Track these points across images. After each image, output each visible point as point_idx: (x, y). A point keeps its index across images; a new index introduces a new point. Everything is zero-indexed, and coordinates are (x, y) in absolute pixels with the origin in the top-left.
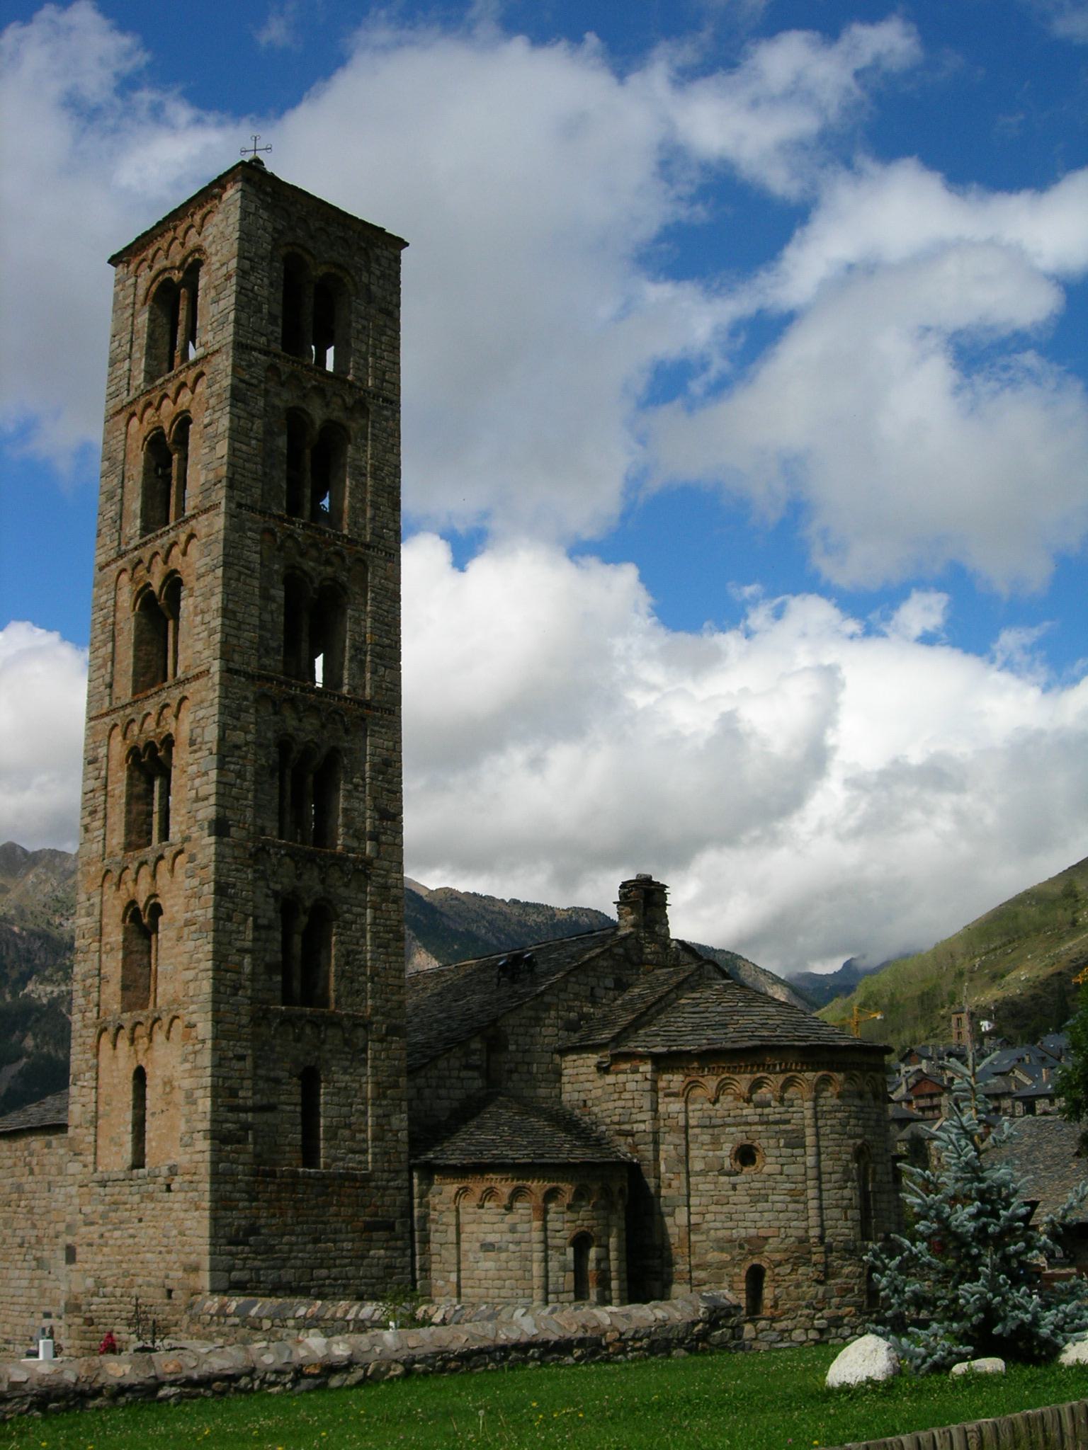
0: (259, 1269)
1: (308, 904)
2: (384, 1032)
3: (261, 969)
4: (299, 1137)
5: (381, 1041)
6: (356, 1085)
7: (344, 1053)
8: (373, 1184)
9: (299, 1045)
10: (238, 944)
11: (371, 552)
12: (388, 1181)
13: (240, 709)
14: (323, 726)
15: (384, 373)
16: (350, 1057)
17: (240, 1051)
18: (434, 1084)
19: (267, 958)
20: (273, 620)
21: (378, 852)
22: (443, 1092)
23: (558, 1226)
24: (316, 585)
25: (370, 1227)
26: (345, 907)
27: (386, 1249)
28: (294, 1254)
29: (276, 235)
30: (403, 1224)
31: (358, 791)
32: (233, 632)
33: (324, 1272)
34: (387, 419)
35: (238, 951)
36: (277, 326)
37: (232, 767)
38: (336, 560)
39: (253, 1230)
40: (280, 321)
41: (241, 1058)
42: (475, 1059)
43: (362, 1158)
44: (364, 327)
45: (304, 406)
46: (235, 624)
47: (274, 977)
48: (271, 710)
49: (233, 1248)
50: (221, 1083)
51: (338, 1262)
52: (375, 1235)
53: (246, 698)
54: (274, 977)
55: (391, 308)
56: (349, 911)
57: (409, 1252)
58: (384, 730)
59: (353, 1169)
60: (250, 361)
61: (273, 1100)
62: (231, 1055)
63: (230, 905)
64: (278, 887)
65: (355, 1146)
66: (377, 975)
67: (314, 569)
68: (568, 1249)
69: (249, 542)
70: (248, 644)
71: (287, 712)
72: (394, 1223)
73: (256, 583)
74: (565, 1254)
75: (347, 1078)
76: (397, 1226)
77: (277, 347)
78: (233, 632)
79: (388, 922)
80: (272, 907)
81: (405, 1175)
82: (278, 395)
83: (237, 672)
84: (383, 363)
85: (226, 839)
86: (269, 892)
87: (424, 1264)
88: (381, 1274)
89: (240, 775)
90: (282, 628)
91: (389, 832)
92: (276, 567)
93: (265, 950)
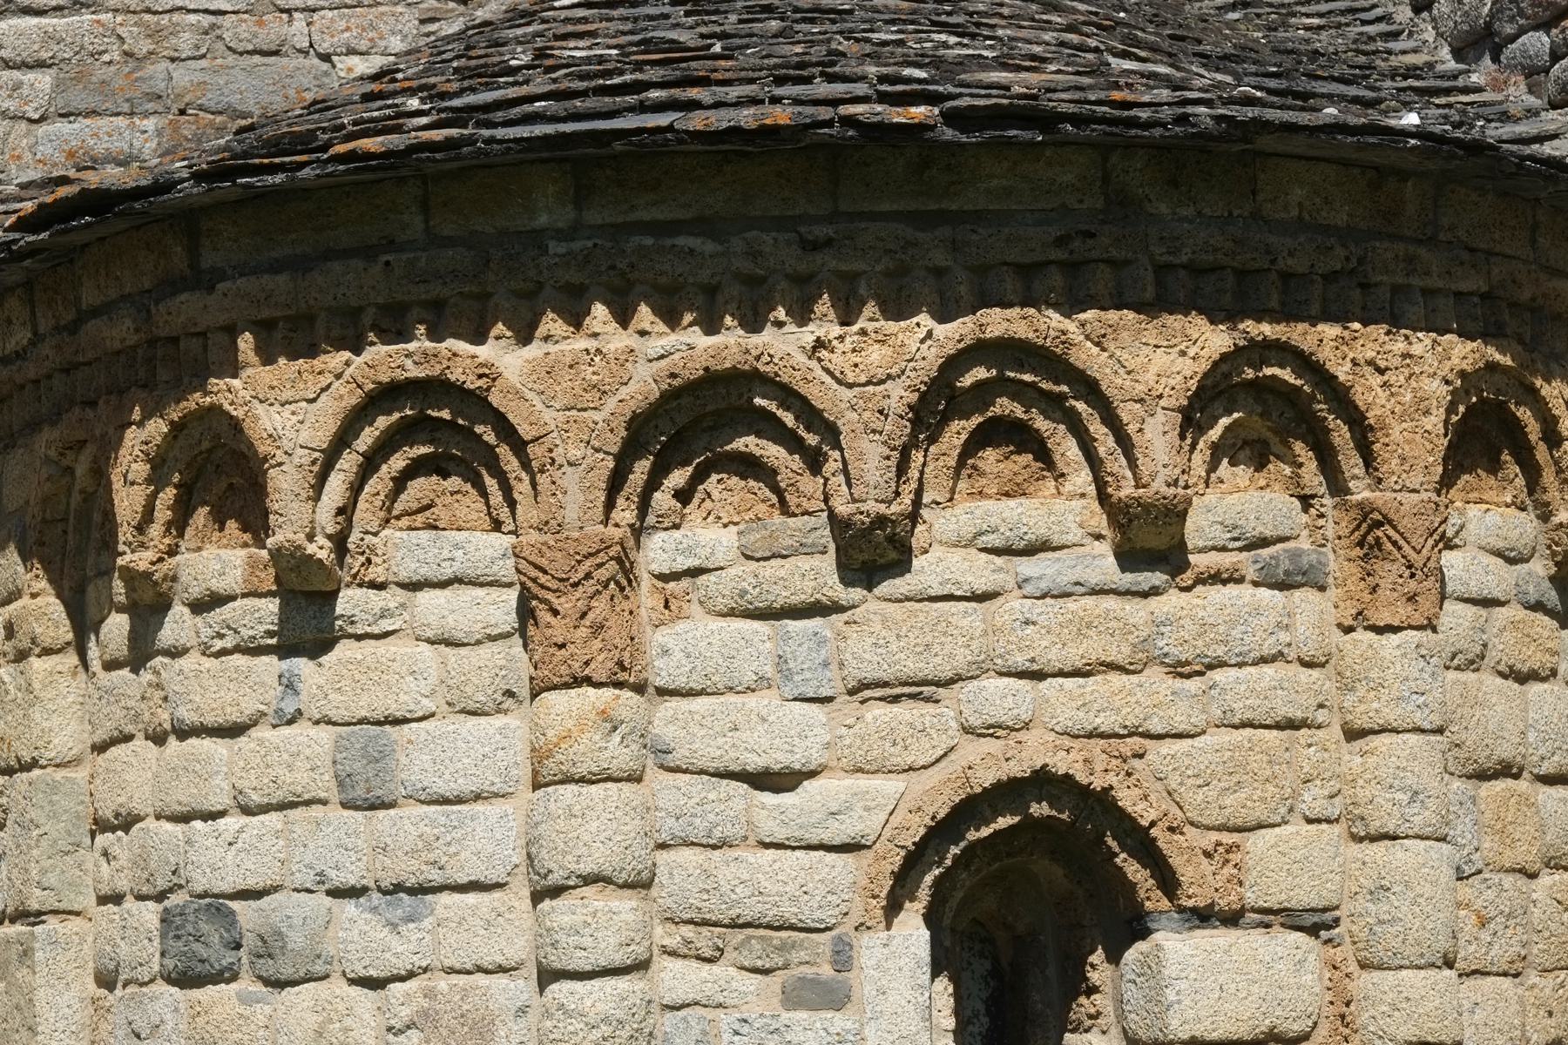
68: (871, 949)
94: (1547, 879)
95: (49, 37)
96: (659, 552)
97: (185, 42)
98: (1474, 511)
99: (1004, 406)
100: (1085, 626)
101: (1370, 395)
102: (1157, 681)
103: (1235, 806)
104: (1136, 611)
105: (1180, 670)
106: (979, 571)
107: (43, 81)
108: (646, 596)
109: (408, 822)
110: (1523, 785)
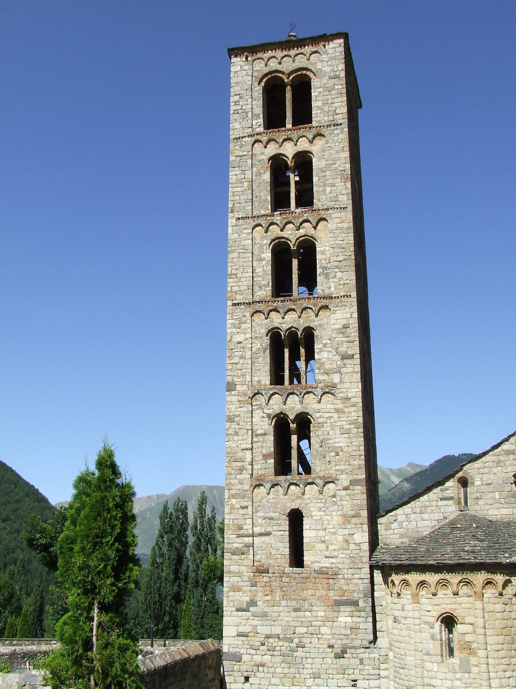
0: (256, 626)
1: (292, 417)
2: (348, 484)
3: (261, 457)
4: (288, 550)
5: (346, 489)
6: (329, 518)
7: (319, 499)
8: (340, 576)
9: (286, 497)
10: (243, 447)
11: (330, 211)
12: (353, 574)
13: (241, 323)
14: (300, 317)
15: (335, 111)
16: (323, 501)
17: (246, 504)
18: (418, 511)
19: (264, 451)
20: (263, 270)
21: (341, 379)
22: (425, 516)
23: (429, 608)
24: (293, 243)
25: (339, 603)
26: (318, 415)
27: (352, 617)
28: (279, 618)
29: (255, 74)
30: (365, 602)
31: (326, 347)
32: (235, 284)
33: (304, 630)
34: (338, 134)
35: (242, 450)
36: (260, 118)
37: (236, 354)
38: (305, 225)
39: (253, 603)
40: (261, 116)
41: (246, 507)
42: (449, 493)
43: (334, 560)
44: (320, 92)
45: (281, 152)
46: (236, 280)
47: (268, 461)
48: (262, 316)
49: (240, 613)
50: (231, 523)
51: (313, 623)
52: (342, 608)
53: (244, 316)
54: (268, 461)
55: (338, 73)
56: (320, 417)
57: (370, 619)
58: (342, 308)
59: (326, 568)
60: (241, 144)
61: (269, 529)
62: (238, 506)
63: (237, 426)
64: (270, 412)
65: (327, 554)
66: (342, 451)
67: (291, 234)
68: (435, 625)
69: (245, 236)
70: (246, 288)
71: (273, 314)
72: (357, 601)
73: (251, 255)
74: (432, 628)
75: (323, 513)
76: (361, 603)
77: (261, 129)
78: (235, 284)
79: (350, 419)
80: (266, 423)
81: (367, 570)
82: (262, 153)
83: (238, 304)
84: (334, 105)
85: (233, 393)
86: (265, 415)
87: (381, 627)
88: (348, 632)
89: (241, 357)
90: (270, 272)
91: (349, 366)
92: (265, 242)
93: (262, 447)
94: (497, 621)
95: (399, 531)
96: (421, 593)
97: (410, 531)
98: (488, 590)
99: (444, 583)
100: (450, 601)
101: (475, 582)
102: (457, 605)
103: (463, 615)
104: (454, 599)
105: (459, 604)
106: (443, 596)
107: (398, 535)
108: (420, 597)
109: (406, 612)
110: (494, 613)
